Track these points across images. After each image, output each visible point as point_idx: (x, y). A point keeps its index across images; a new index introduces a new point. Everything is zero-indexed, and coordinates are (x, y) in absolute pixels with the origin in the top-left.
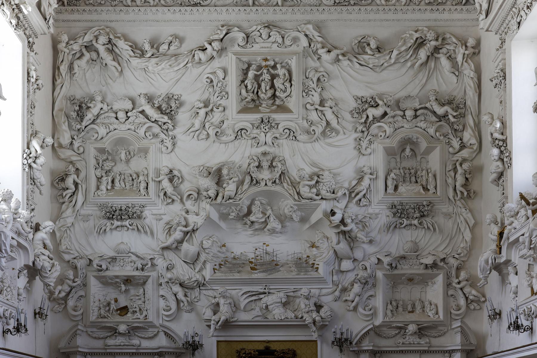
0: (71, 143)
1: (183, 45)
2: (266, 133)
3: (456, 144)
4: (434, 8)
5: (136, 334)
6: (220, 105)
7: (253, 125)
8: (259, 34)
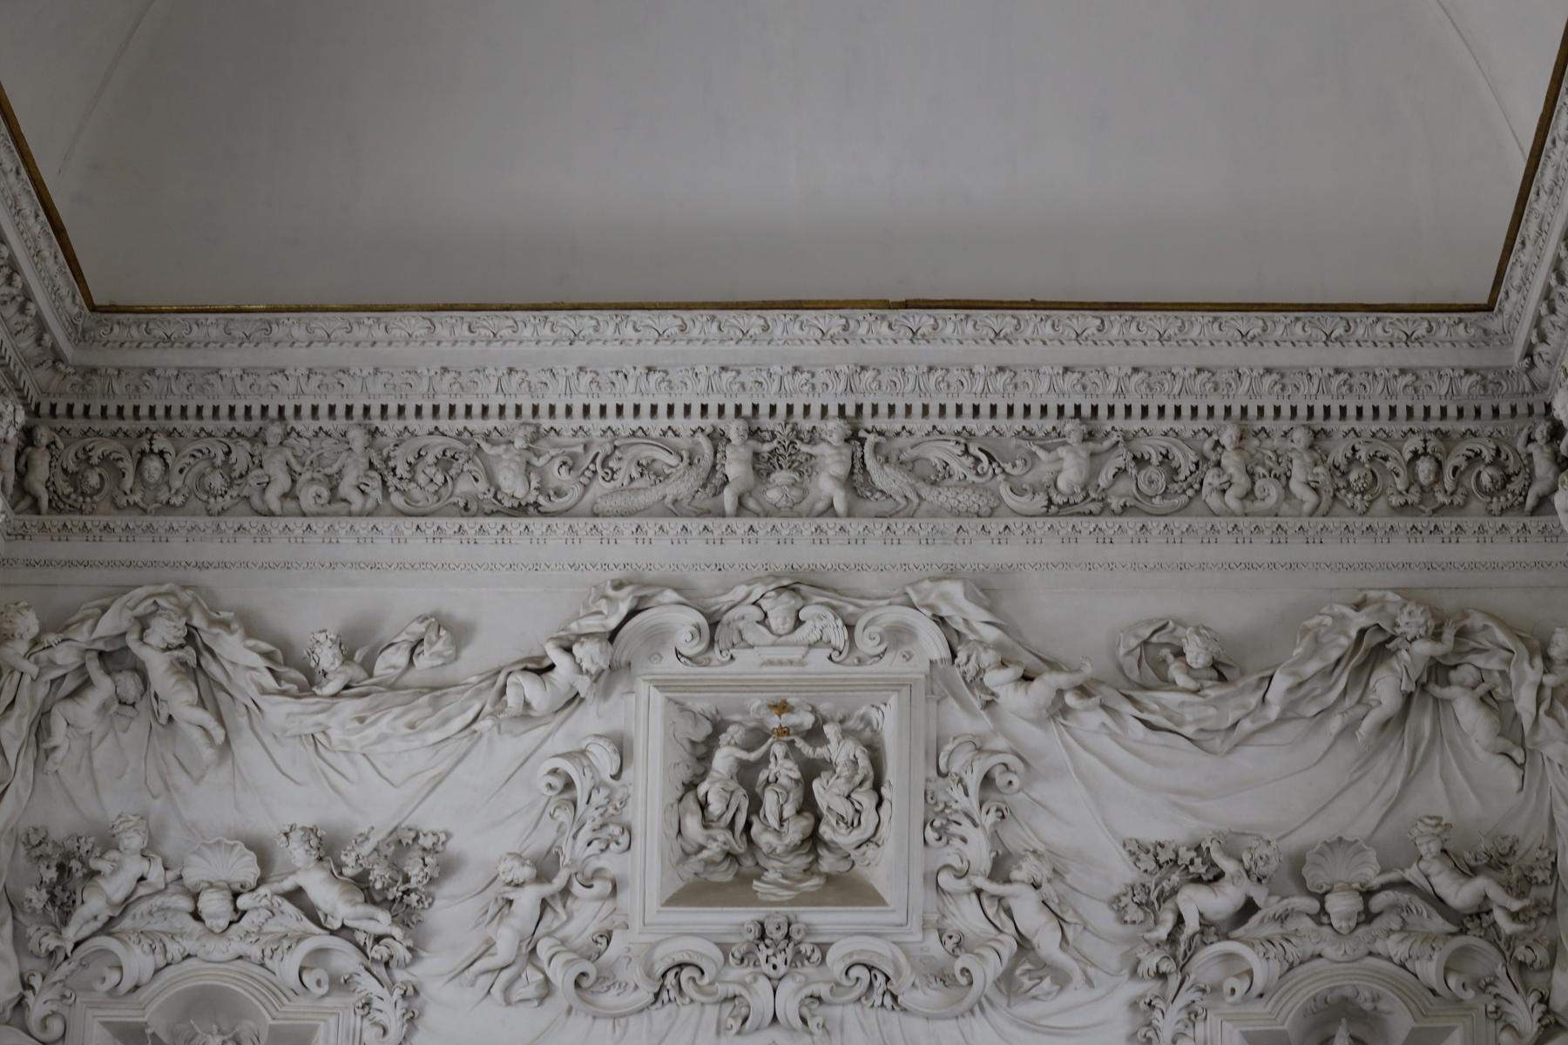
0: (20, 1004)
1: (466, 653)
2: (775, 984)
4: (1422, 522)
6: (597, 873)
7: (725, 949)
8: (756, 614)
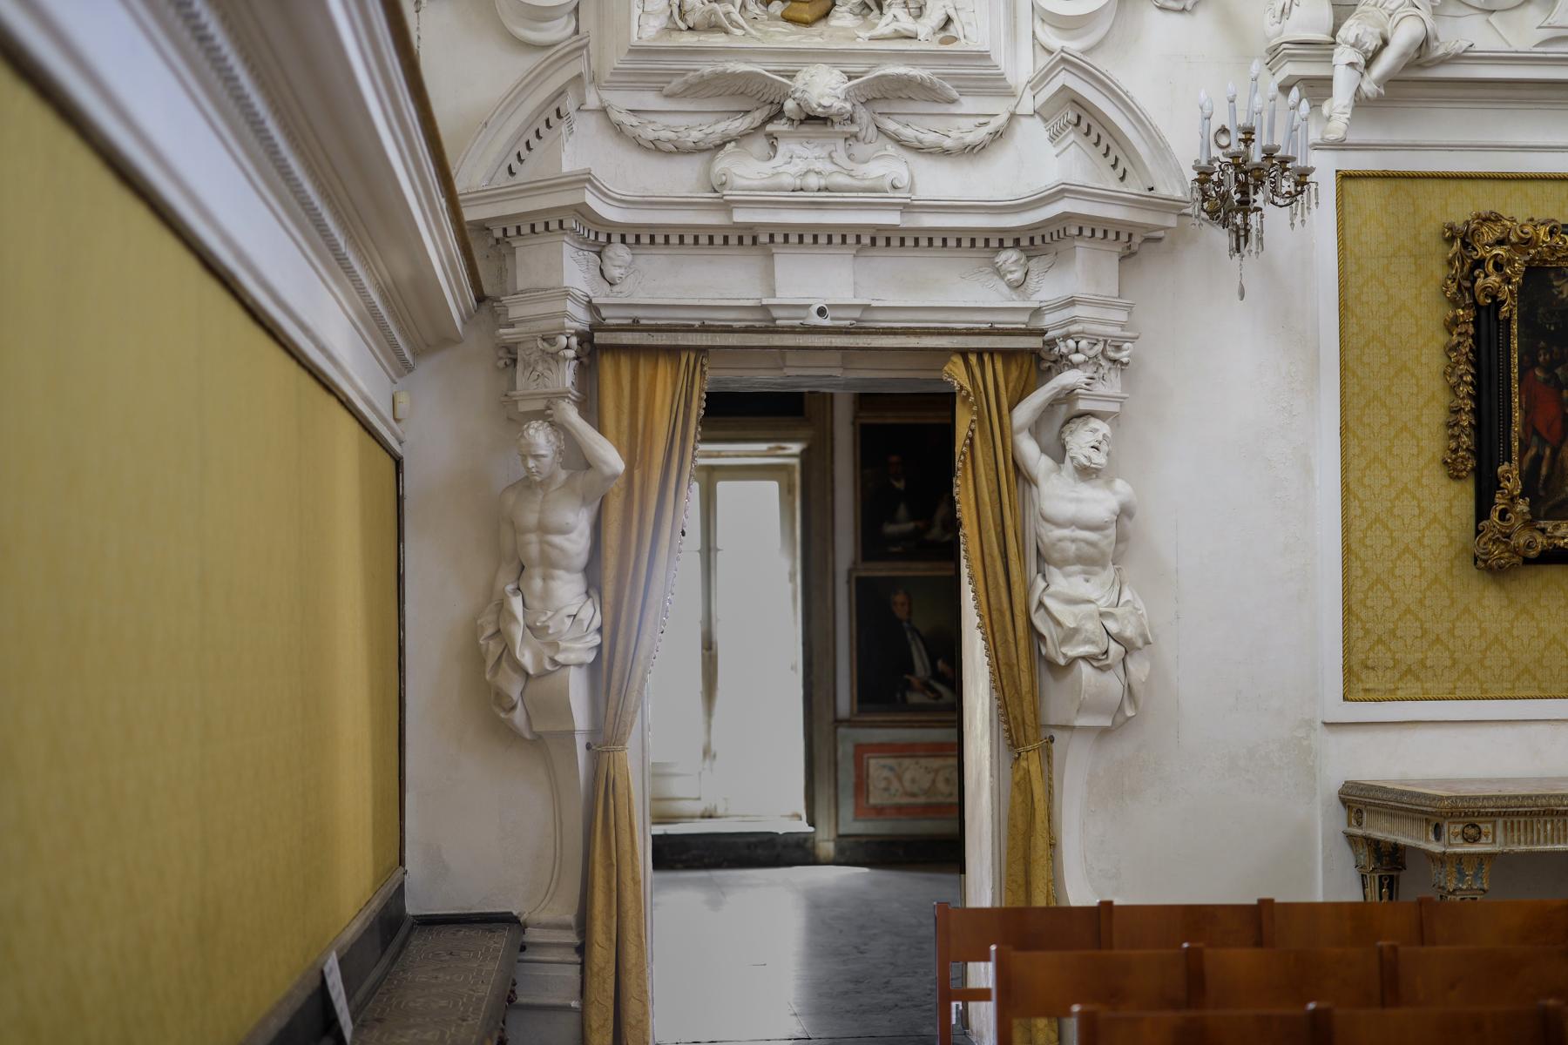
5: (891, 125)
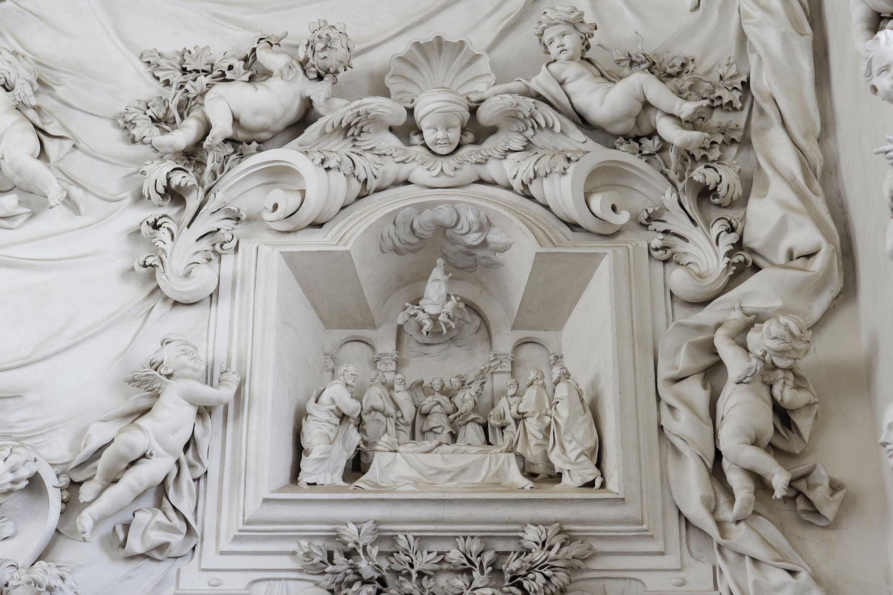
3: (706, 253)
